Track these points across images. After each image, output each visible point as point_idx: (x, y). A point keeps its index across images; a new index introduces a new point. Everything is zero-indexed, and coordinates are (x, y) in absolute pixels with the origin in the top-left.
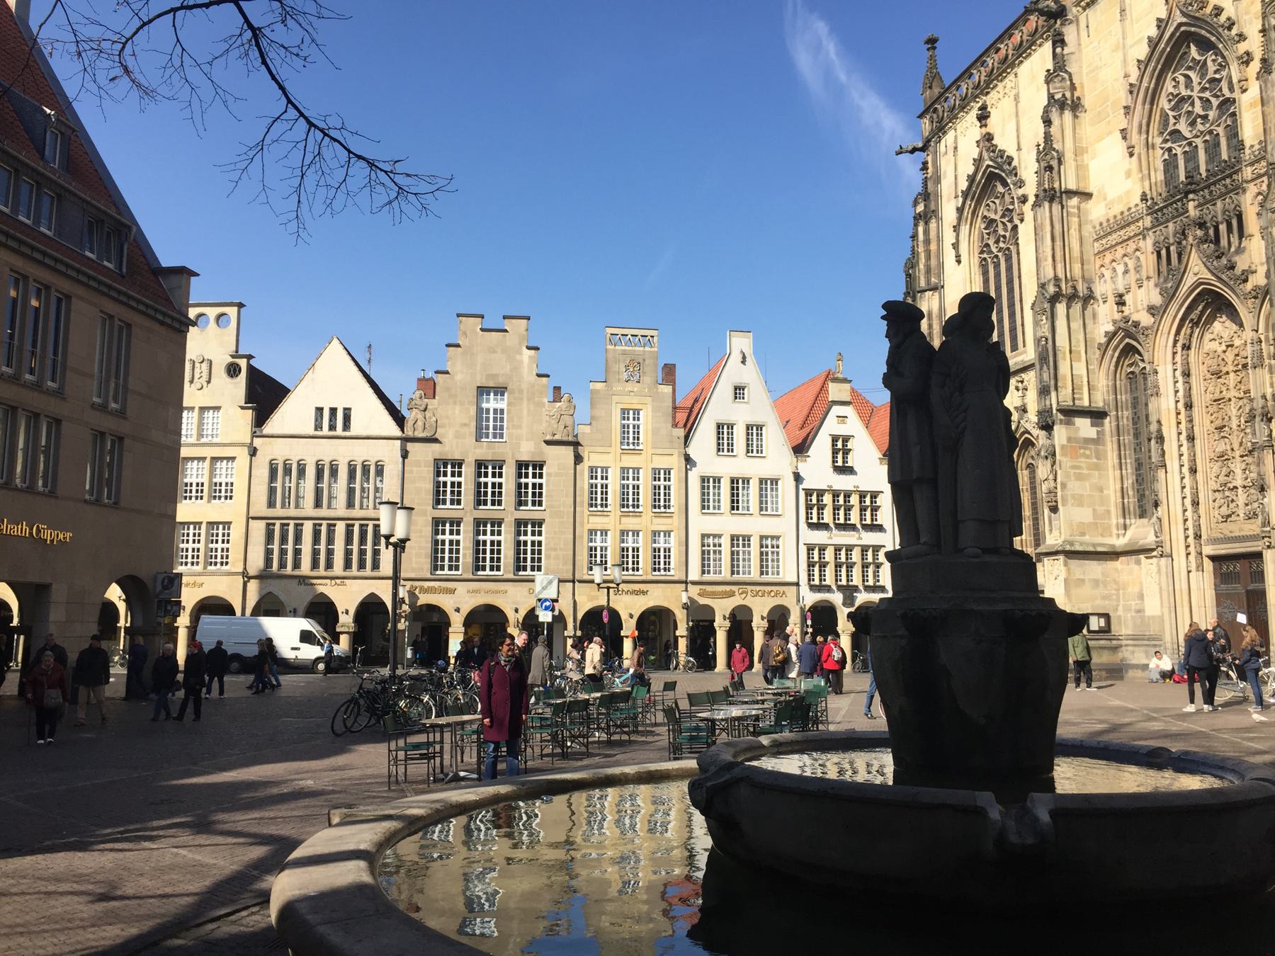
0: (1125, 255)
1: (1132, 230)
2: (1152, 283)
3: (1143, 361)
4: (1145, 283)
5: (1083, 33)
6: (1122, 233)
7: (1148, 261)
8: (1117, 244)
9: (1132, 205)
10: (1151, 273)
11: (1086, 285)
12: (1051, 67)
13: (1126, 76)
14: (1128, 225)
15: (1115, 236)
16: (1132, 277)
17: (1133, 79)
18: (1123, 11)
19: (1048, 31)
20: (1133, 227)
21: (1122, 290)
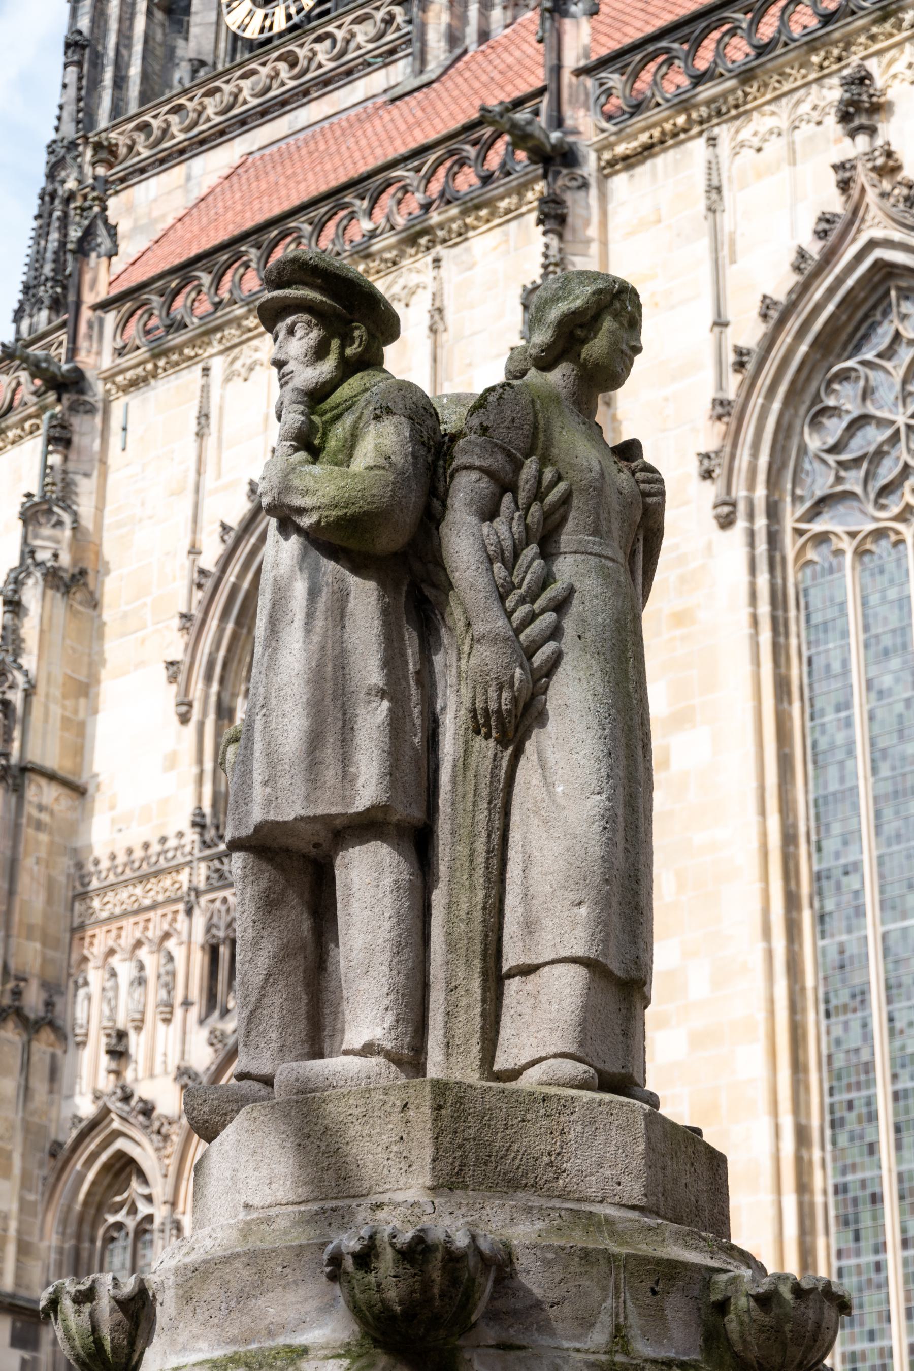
0: (139, 944)
1: (157, 890)
2: (194, 1013)
3: (149, 1199)
4: (179, 1012)
5: (115, 440)
6: (138, 890)
7: (191, 966)
8: (125, 914)
9: (171, 832)
10: (195, 994)
11: (43, 996)
12: (35, 489)
13: (194, 551)
14: (157, 874)
15: (124, 894)
16: (154, 994)
17: (209, 560)
18: (204, 416)
19: (37, 416)
20: (167, 882)
21: (122, 1022)
